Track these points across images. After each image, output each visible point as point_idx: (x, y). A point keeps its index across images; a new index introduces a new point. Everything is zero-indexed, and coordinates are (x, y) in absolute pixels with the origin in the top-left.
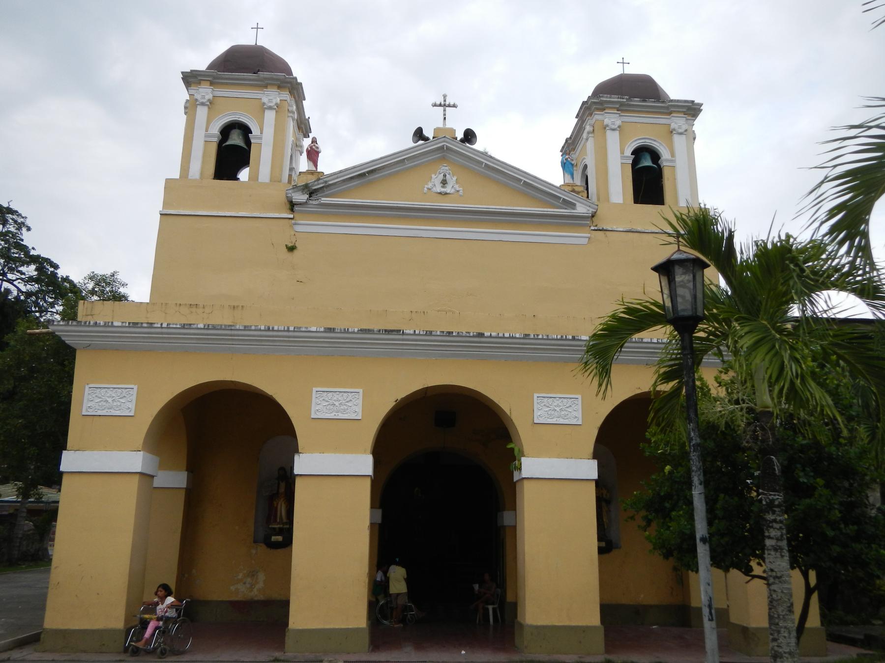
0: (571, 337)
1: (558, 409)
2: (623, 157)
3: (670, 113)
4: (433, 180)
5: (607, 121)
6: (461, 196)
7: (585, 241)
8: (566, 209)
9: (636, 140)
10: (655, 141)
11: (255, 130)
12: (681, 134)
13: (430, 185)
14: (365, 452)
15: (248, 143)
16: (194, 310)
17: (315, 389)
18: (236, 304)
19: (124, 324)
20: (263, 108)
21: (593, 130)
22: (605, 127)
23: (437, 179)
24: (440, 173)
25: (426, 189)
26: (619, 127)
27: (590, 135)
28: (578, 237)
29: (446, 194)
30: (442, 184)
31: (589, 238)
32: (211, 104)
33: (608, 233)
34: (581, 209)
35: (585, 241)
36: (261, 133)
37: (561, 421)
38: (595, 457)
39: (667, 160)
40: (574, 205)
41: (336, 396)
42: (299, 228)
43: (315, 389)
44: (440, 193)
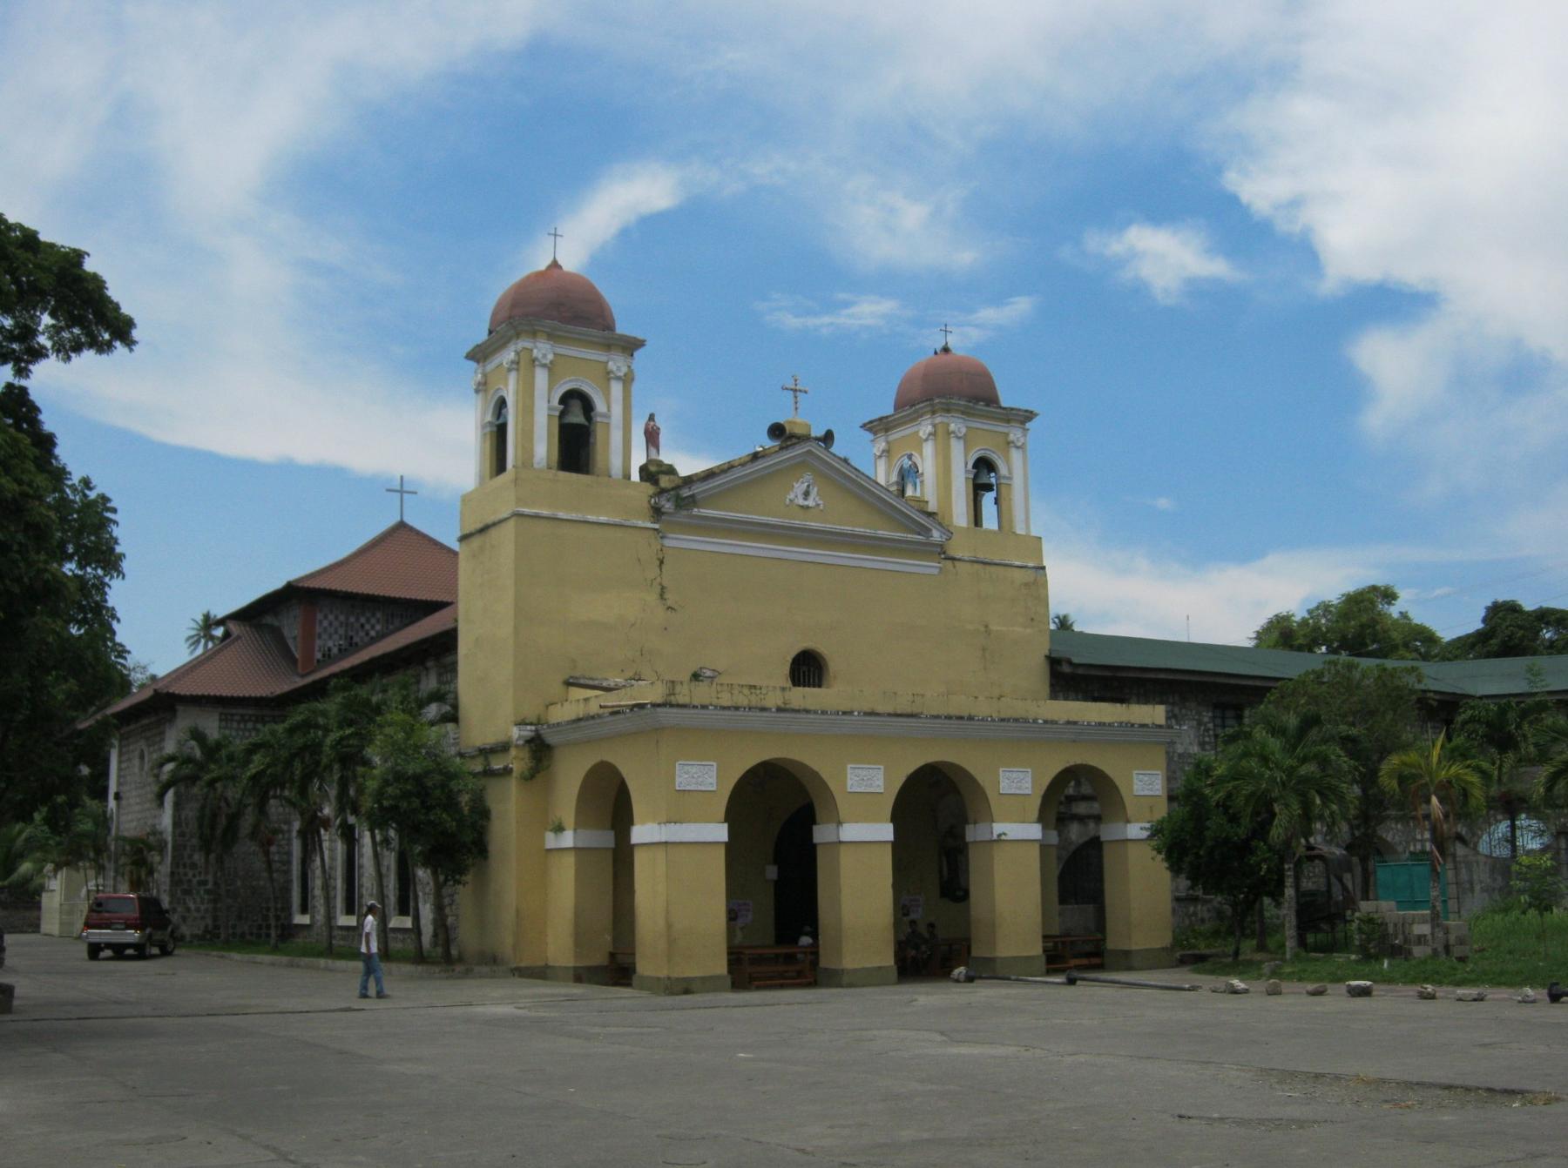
2: (967, 472)
3: (1008, 421)
4: (795, 490)
5: (952, 427)
6: (822, 511)
7: (936, 571)
8: (919, 534)
9: (979, 450)
10: (994, 452)
11: (600, 406)
12: (1018, 447)
13: (792, 496)
14: (886, 822)
16: (753, 691)
17: (849, 766)
20: (608, 376)
21: (935, 431)
22: (949, 433)
23: (800, 488)
24: (803, 483)
25: (788, 500)
26: (965, 435)
27: (931, 437)
28: (929, 567)
29: (808, 507)
31: (940, 568)
32: (550, 368)
33: (957, 563)
34: (936, 535)
35: (936, 571)
36: (609, 410)
37: (1018, 792)
39: (1005, 477)
40: (930, 530)
41: (865, 773)
42: (667, 543)
43: (849, 766)
44: (802, 507)
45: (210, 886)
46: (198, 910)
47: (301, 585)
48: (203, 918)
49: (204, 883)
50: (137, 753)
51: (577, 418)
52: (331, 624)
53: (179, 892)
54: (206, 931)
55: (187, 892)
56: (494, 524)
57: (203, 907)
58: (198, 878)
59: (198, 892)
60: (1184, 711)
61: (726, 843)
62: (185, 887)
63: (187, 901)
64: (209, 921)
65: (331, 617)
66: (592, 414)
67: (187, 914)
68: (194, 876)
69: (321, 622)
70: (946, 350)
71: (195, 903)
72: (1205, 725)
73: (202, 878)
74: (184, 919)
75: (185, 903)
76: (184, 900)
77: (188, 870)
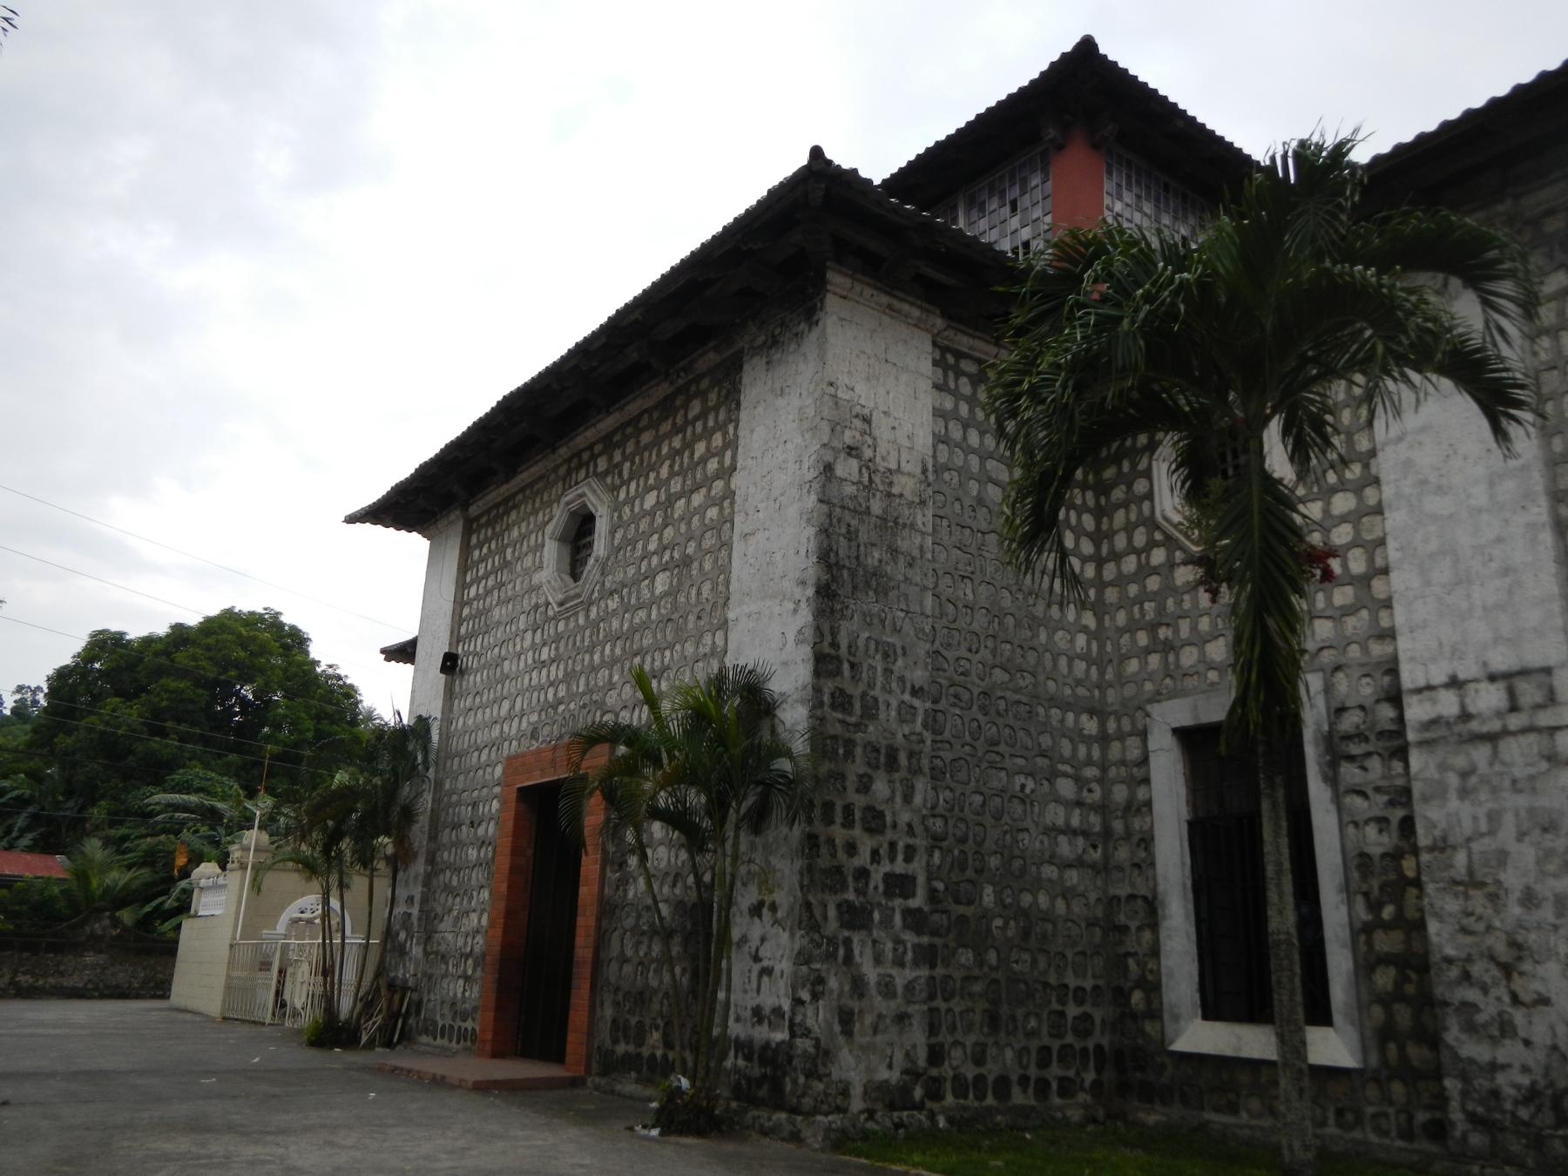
45: (918, 901)
46: (887, 989)
48: (902, 1018)
49: (899, 885)
50: (558, 517)
53: (832, 912)
54: (912, 1073)
55: (855, 917)
57: (901, 977)
58: (886, 867)
59: (887, 922)
62: (851, 896)
64: (917, 1036)
67: (855, 1005)
68: (875, 855)
71: (878, 960)
73: (899, 867)
74: (846, 1019)
75: (849, 958)
76: (848, 942)
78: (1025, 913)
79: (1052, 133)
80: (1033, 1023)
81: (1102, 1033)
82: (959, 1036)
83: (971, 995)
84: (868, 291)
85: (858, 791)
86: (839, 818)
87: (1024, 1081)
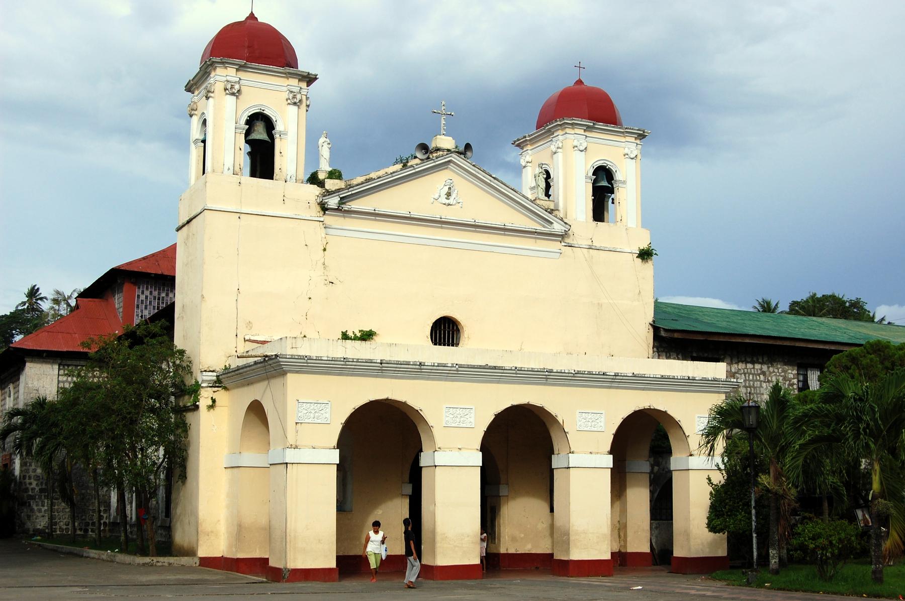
0: (602, 373)
1: (590, 420)
15: (272, 137)
18: (391, 342)
19: (329, 359)
30: (446, 196)
38: (611, 452)
47: (122, 268)
51: (260, 134)
52: (146, 297)
56: (195, 217)
60: (771, 369)
61: (481, 466)
63: (32, 503)
65: (147, 293)
66: (273, 132)
69: (139, 296)
70: (579, 82)
72: (790, 381)
76: (29, 502)
77: (32, 480)
78: (83, 494)
79: (119, 281)
80: (84, 517)
81: (106, 519)
82: (61, 520)
83: (65, 512)
84: (36, 360)
85: (32, 472)
86: (27, 478)
87: (80, 529)
